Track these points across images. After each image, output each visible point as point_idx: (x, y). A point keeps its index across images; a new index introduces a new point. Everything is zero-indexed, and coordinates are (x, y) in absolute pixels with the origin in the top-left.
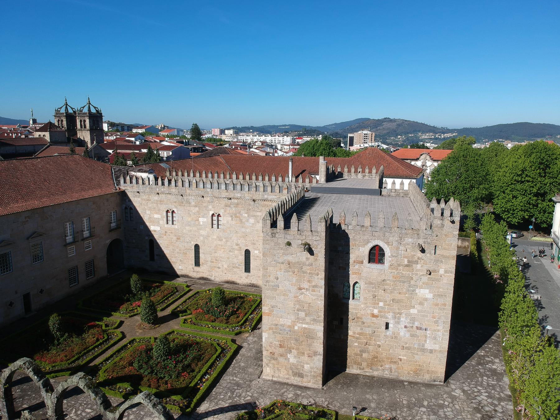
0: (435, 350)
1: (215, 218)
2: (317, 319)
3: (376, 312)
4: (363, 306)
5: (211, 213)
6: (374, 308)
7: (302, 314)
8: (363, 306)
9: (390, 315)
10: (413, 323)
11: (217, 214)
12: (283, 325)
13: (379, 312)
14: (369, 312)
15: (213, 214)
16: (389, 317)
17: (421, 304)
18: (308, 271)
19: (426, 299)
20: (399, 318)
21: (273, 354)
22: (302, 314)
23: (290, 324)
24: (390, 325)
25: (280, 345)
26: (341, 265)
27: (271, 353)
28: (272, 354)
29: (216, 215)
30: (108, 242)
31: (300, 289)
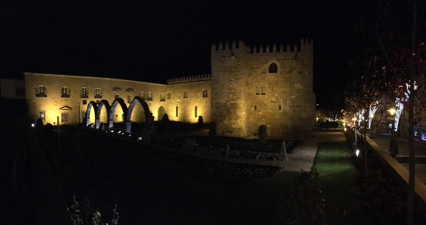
1: (205, 92)
3: (274, 99)
4: (266, 97)
5: (203, 90)
6: (273, 97)
8: (266, 97)
9: (281, 100)
10: (294, 104)
12: (221, 103)
13: (276, 99)
14: (270, 100)
16: (281, 101)
20: (286, 102)
23: (225, 102)
24: (282, 107)
26: (255, 76)
31: (230, 81)
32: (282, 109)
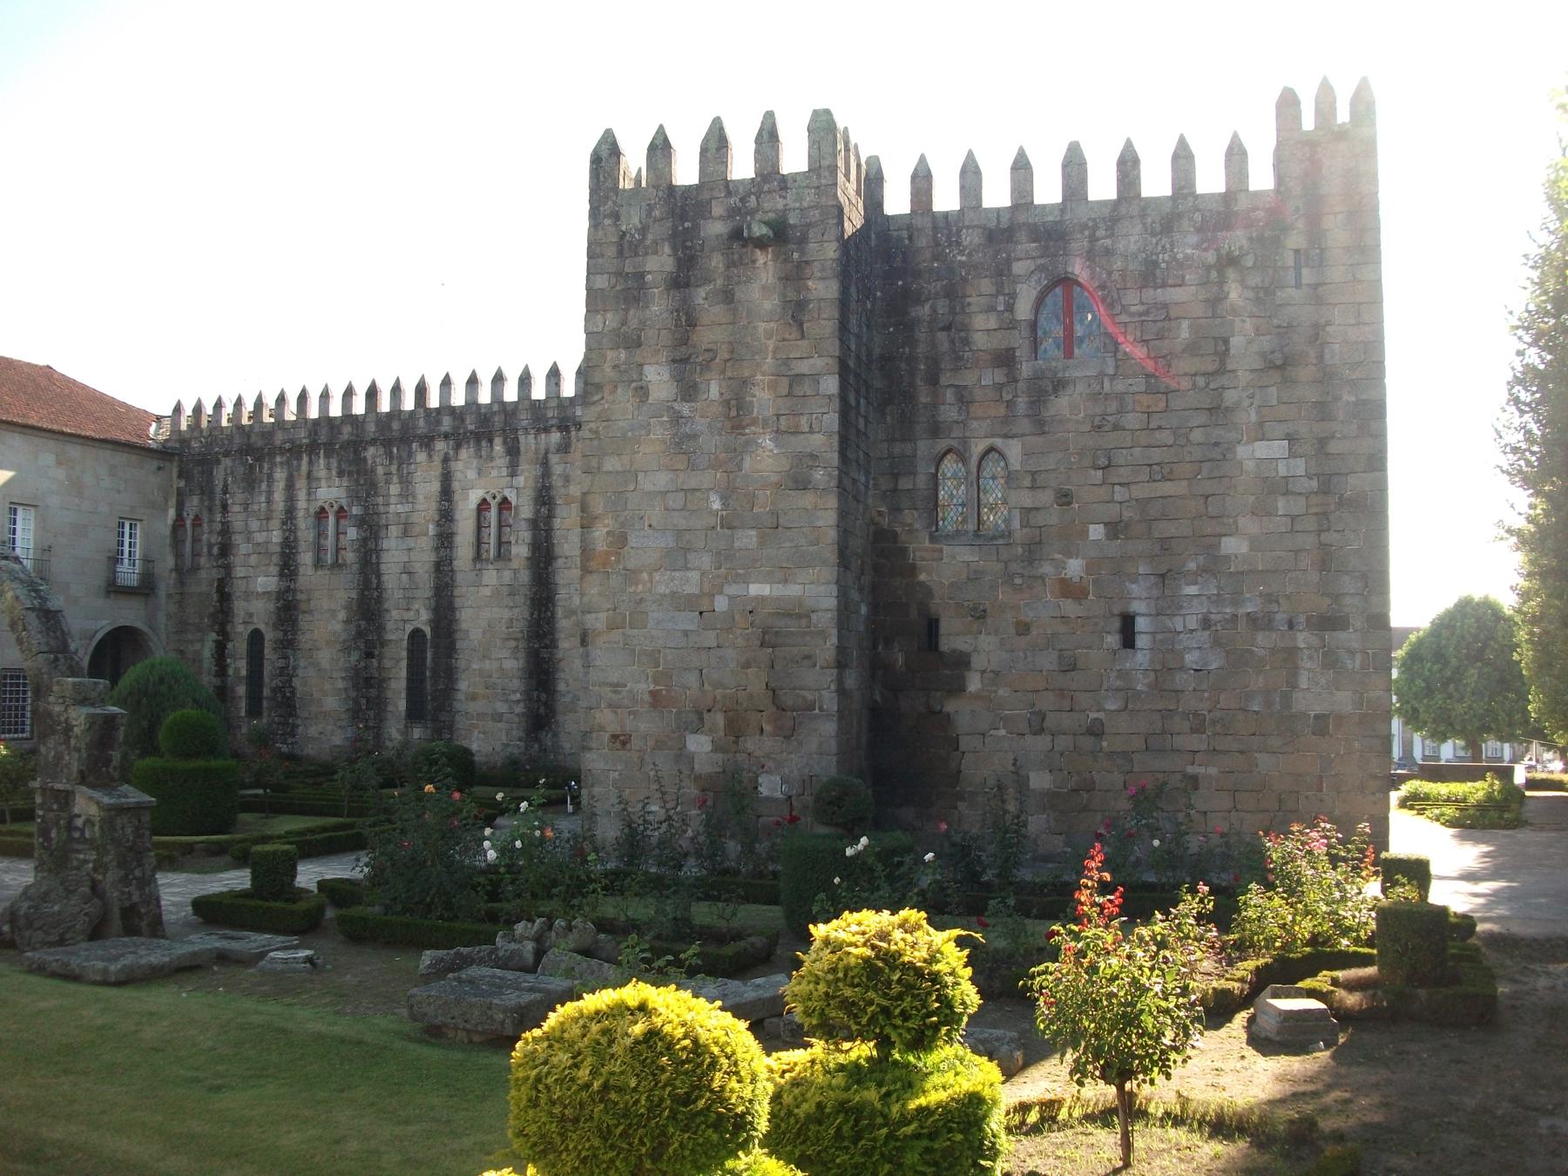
0: (1340, 718)
2: (811, 548)
5: (475, 497)
7: (747, 539)
11: (498, 498)
15: (484, 501)
17: (1262, 511)
18: (771, 344)
19: (1283, 487)
21: (624, 743)
22: (747, 539)
24: (1141, 624)
25: (653, 694)
27: (615, 737)
28: (618, 744)
29: (494, 504)
30: (104, 626)
32: (1142, 641)
